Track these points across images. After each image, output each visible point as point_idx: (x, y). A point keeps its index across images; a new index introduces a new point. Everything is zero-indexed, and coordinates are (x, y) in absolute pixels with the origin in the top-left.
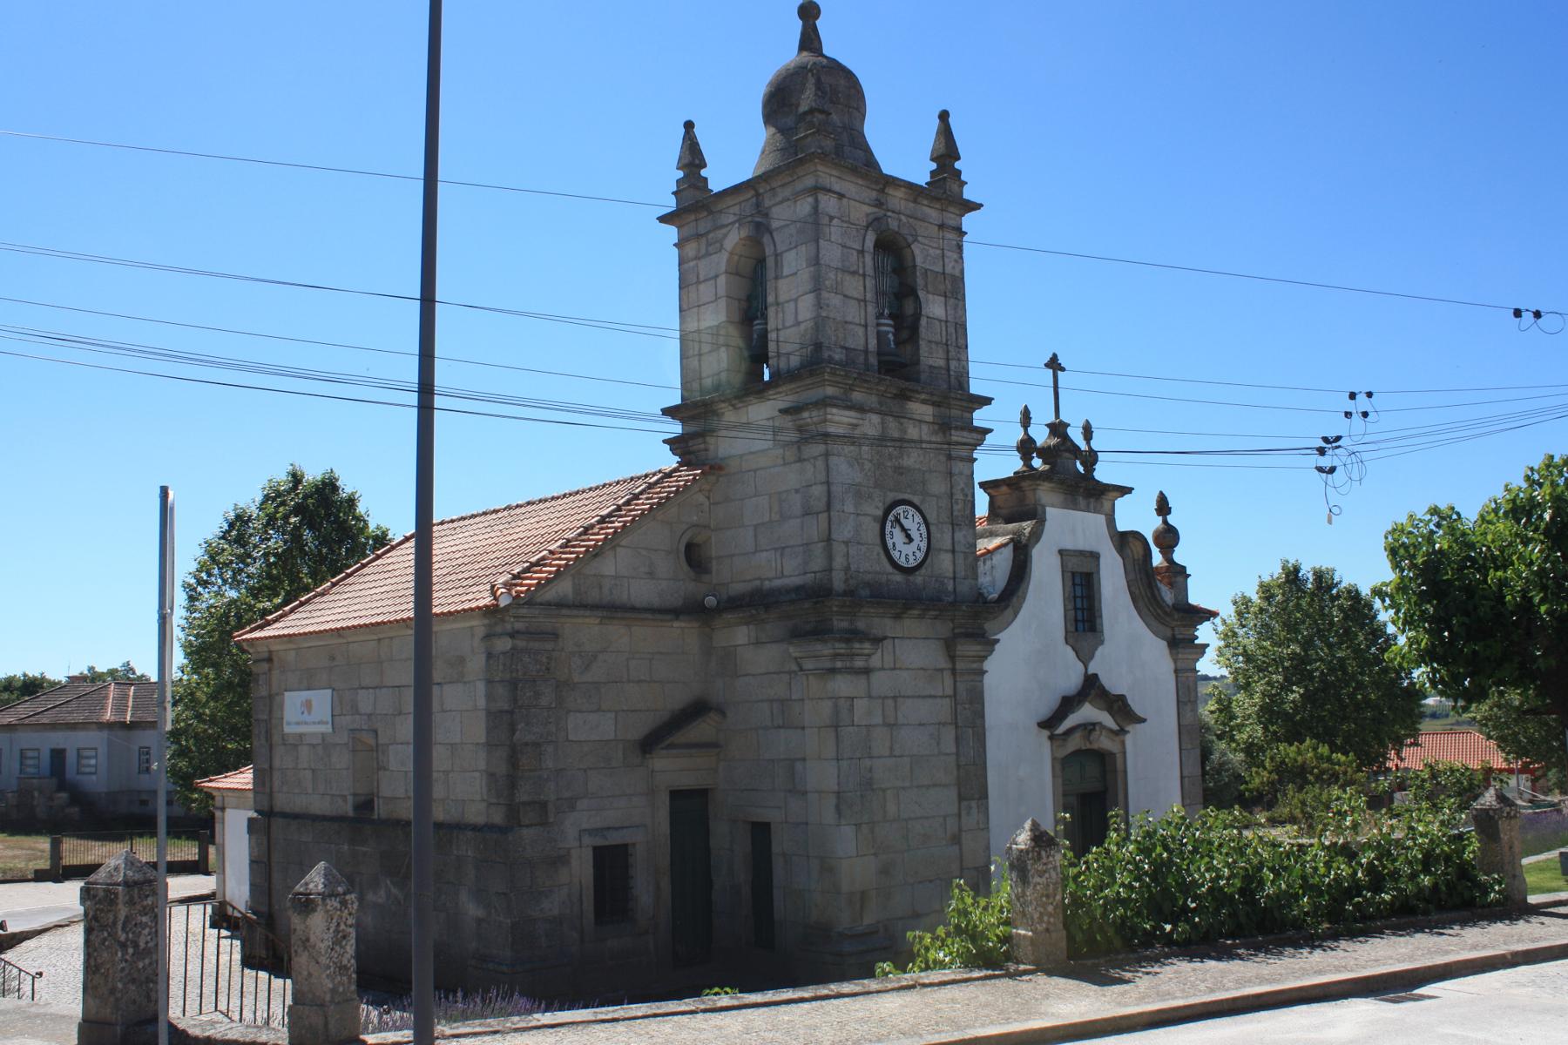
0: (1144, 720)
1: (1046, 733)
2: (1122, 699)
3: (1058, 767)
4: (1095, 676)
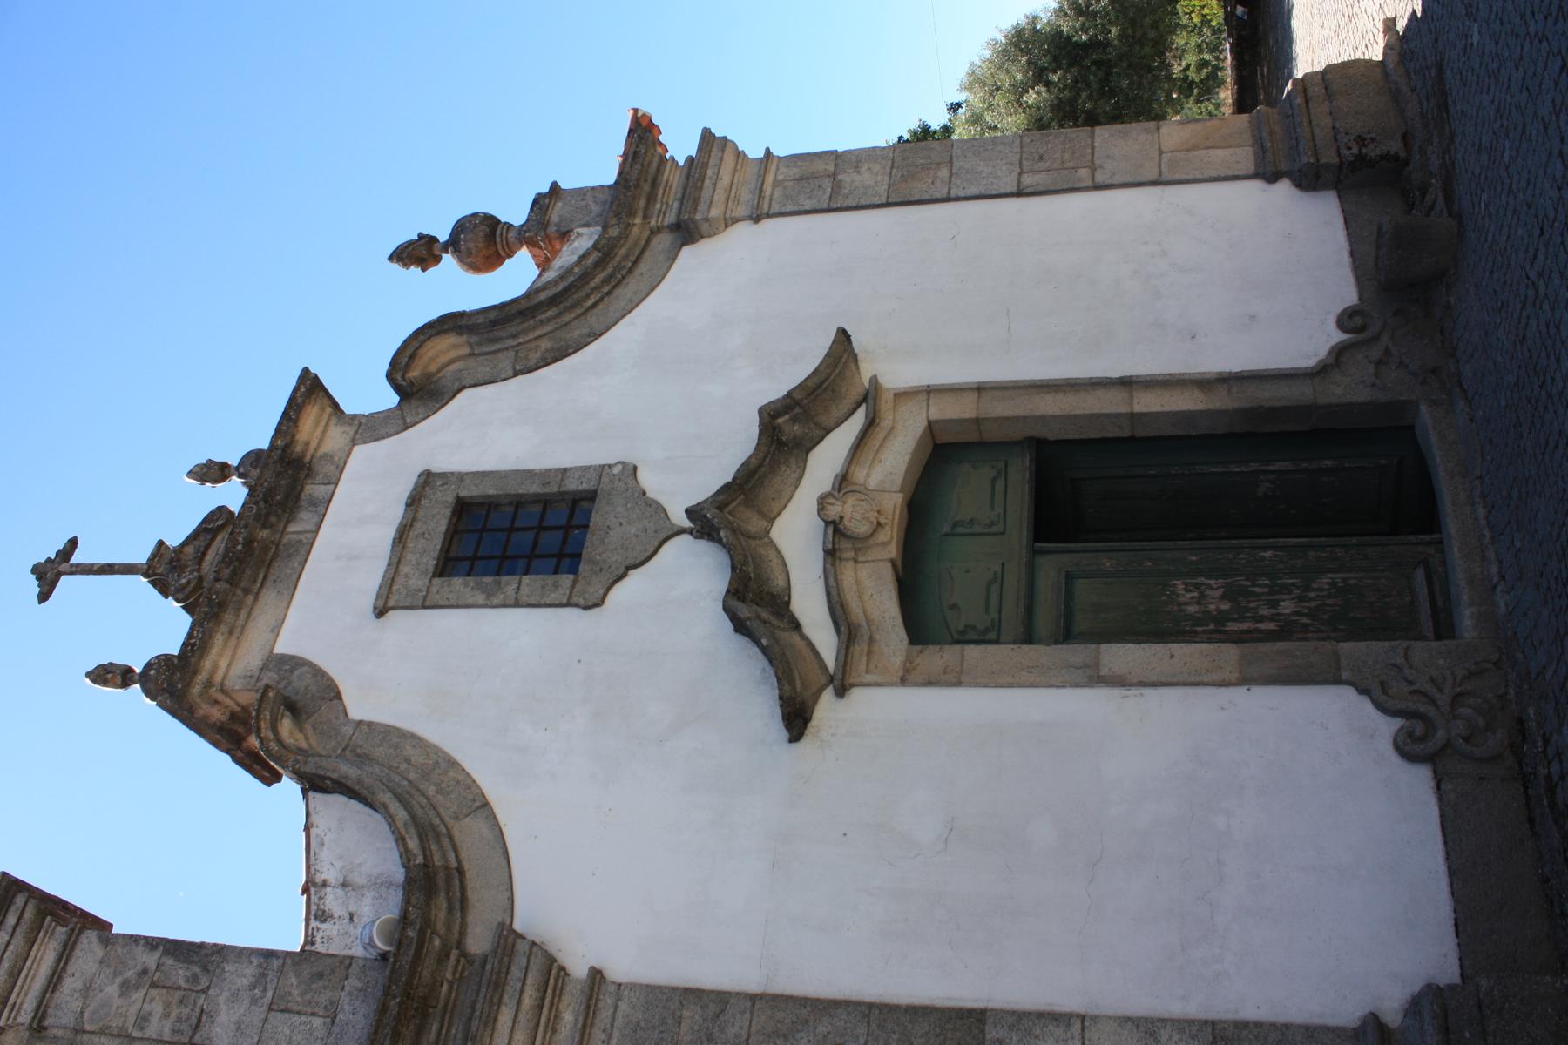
0: (843, 336)
1: (827, 708)
2: (770, 417)
3: (936, 658)
4: (690, 512)
